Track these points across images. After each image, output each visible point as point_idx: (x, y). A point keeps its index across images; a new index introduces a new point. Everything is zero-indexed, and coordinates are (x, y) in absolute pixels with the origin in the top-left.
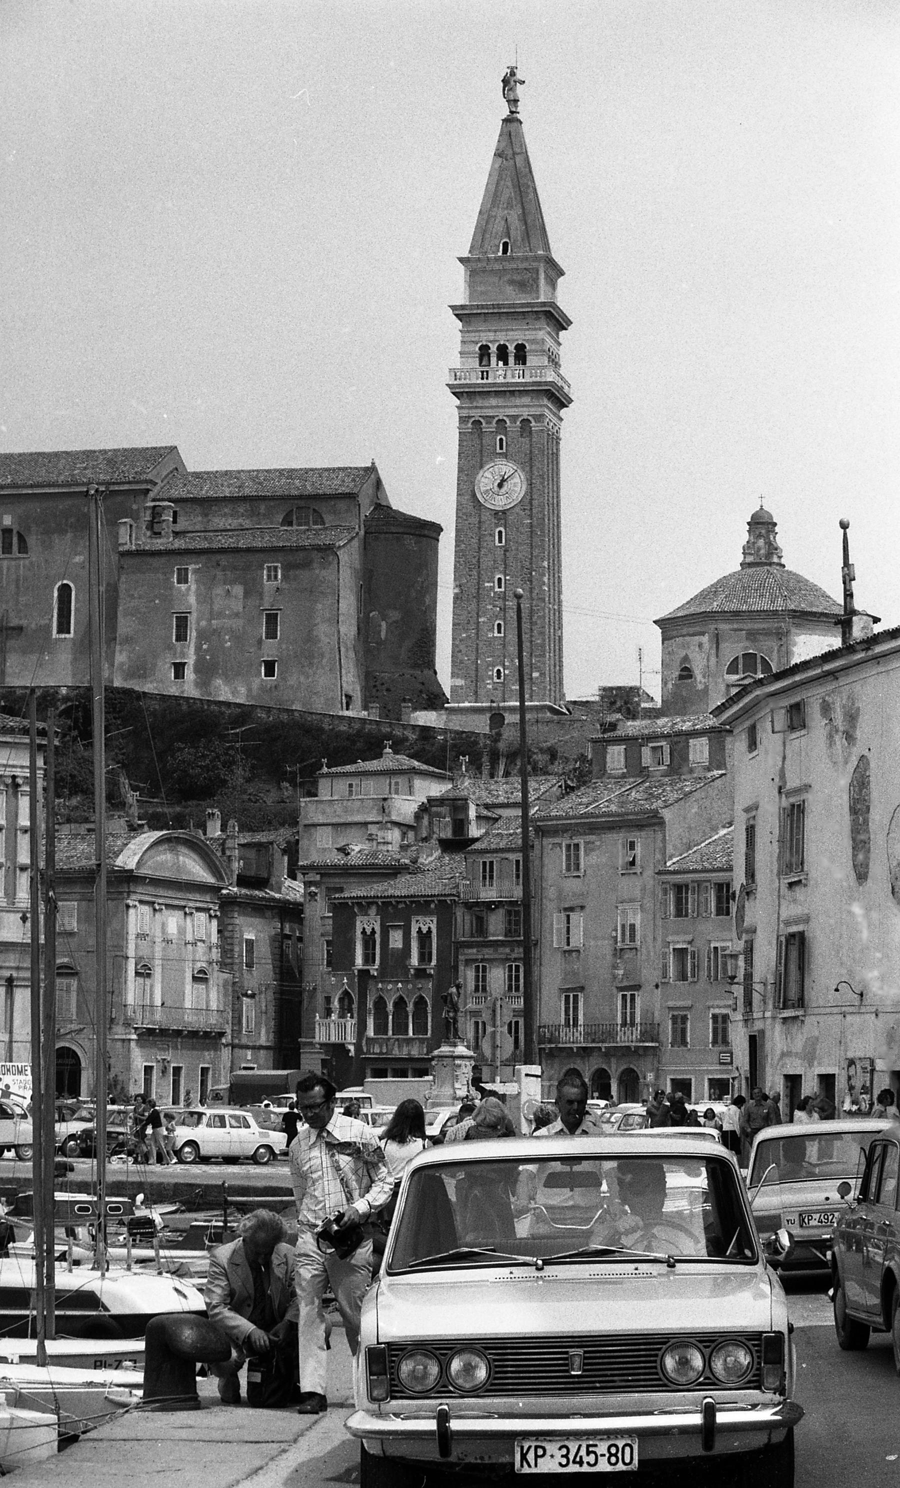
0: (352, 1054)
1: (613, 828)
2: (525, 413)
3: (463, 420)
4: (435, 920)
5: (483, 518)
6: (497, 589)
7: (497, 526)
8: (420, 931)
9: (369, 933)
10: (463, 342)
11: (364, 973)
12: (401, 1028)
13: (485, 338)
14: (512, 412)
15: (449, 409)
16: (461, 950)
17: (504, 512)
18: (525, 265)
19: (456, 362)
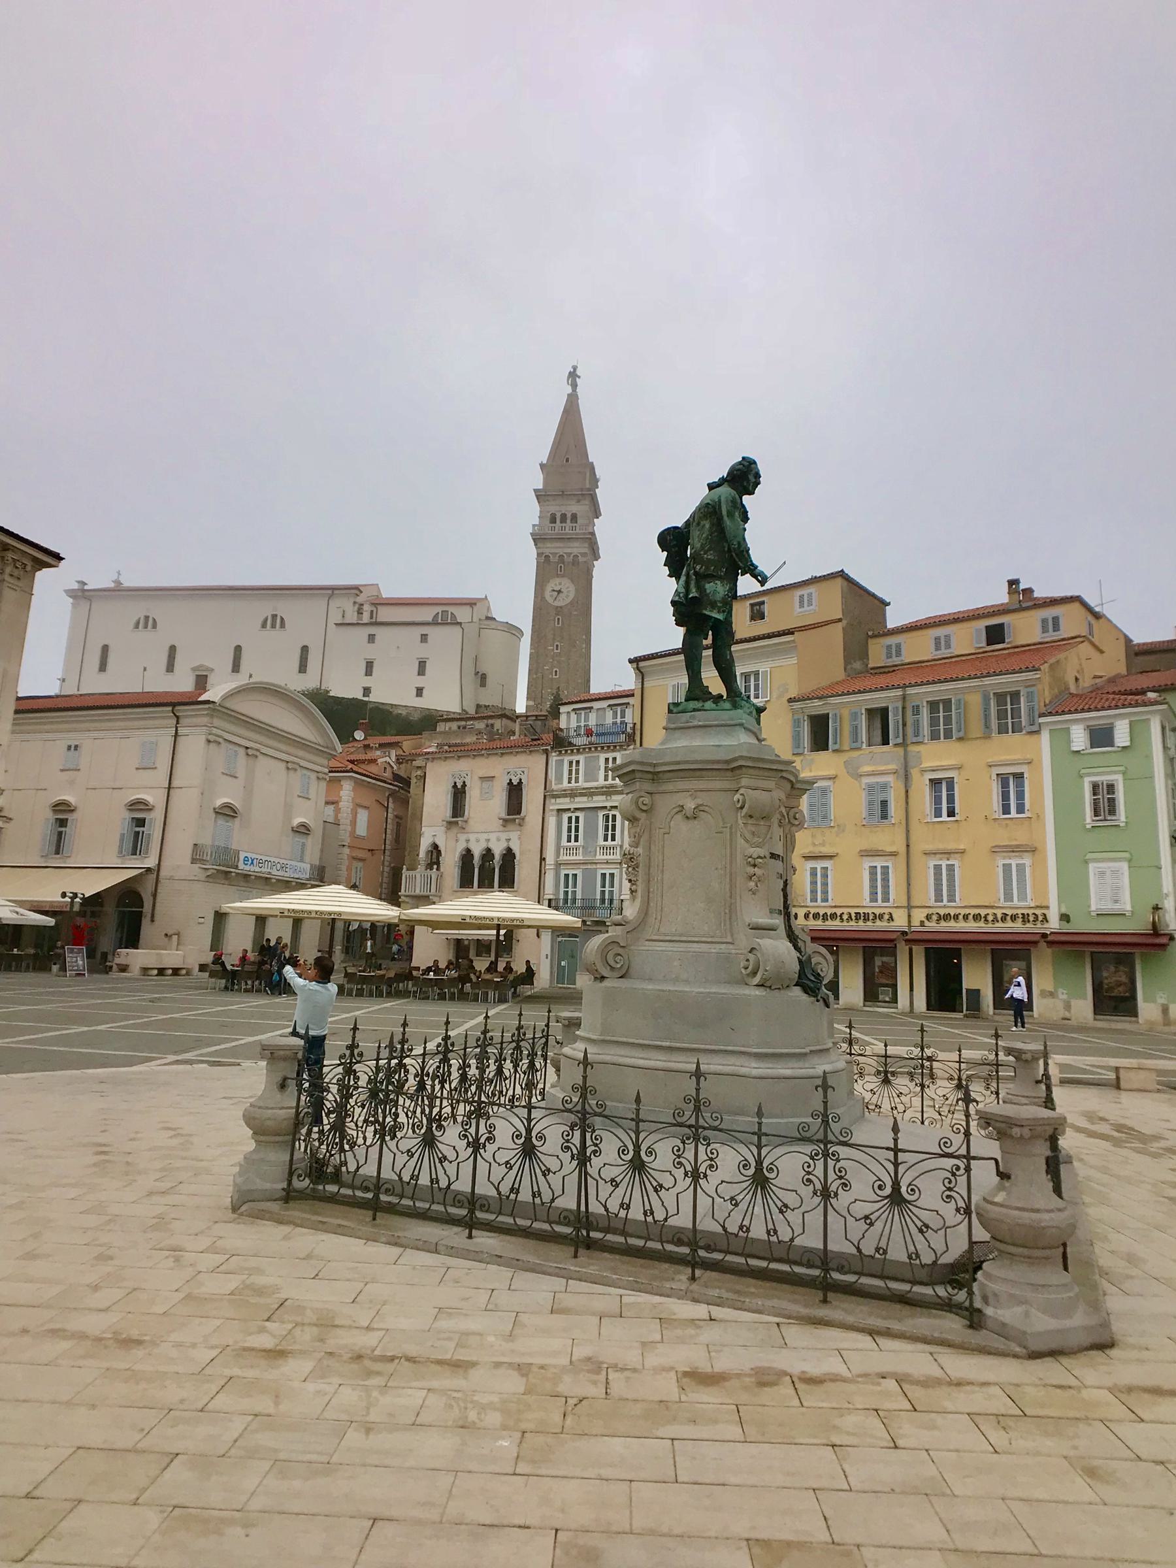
2: (575, 551)
14: (569, 551)
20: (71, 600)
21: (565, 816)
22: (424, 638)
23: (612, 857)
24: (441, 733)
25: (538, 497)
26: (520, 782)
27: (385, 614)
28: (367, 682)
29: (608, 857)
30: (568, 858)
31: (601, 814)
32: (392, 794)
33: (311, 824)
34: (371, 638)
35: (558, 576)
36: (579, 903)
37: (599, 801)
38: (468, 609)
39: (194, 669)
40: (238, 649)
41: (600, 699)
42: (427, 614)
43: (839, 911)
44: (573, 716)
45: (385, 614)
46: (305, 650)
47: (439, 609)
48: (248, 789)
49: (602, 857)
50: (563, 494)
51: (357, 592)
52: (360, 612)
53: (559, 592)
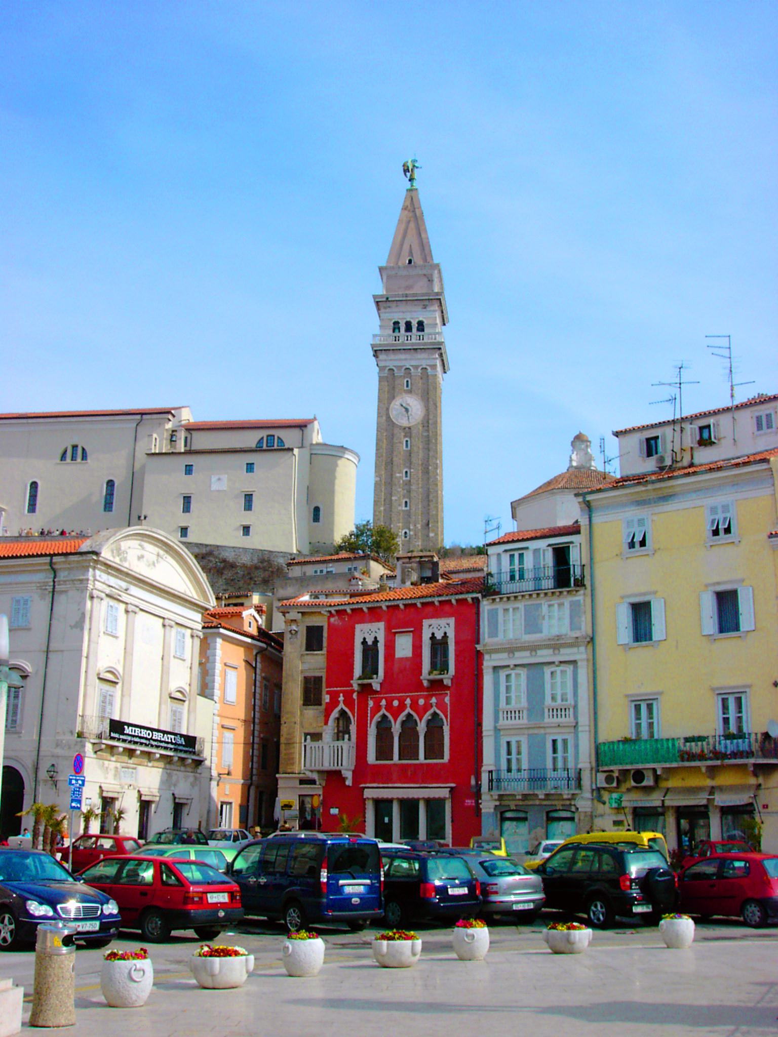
0: (349, 782)
1: (699, 490)
2: (424, 364)
3: (381, 369)
4: (452, 621)
5: (395, 432)
6: (404, 478)
7: (405, 436)
8: (433, 637)
9: (370, 642)
11: (366, 689)
12: (409, 750)
13: (396, 317)
14: (414, 363)
16: (486, 657)
17: (409, 428)
18: (425, 272)
19: (377, 331)
21: (503, 674)
22: (250, 467)
23: (563, 719)
24: (296, 579)
25: (377, 303)
26: (445, 636)
27: (202, 441)
29: (559, 720)
30: (509, 722)
31: (547, 671)
32: (261, 651)
33: (187, 688)
34: (189, 469)
36: (524, 774)
37: (544, 655)
38: (296, 432)
40: (34, 485)
41: (536, 538)
42: (250, 439)
44: (505, 558)
45: (202, 441)
46: (110, 484)
47: (264, 433)
48: (128, 651)
49: (551, 720)
50: (407, 300)
51: (170, 417)
52: (172, 440)
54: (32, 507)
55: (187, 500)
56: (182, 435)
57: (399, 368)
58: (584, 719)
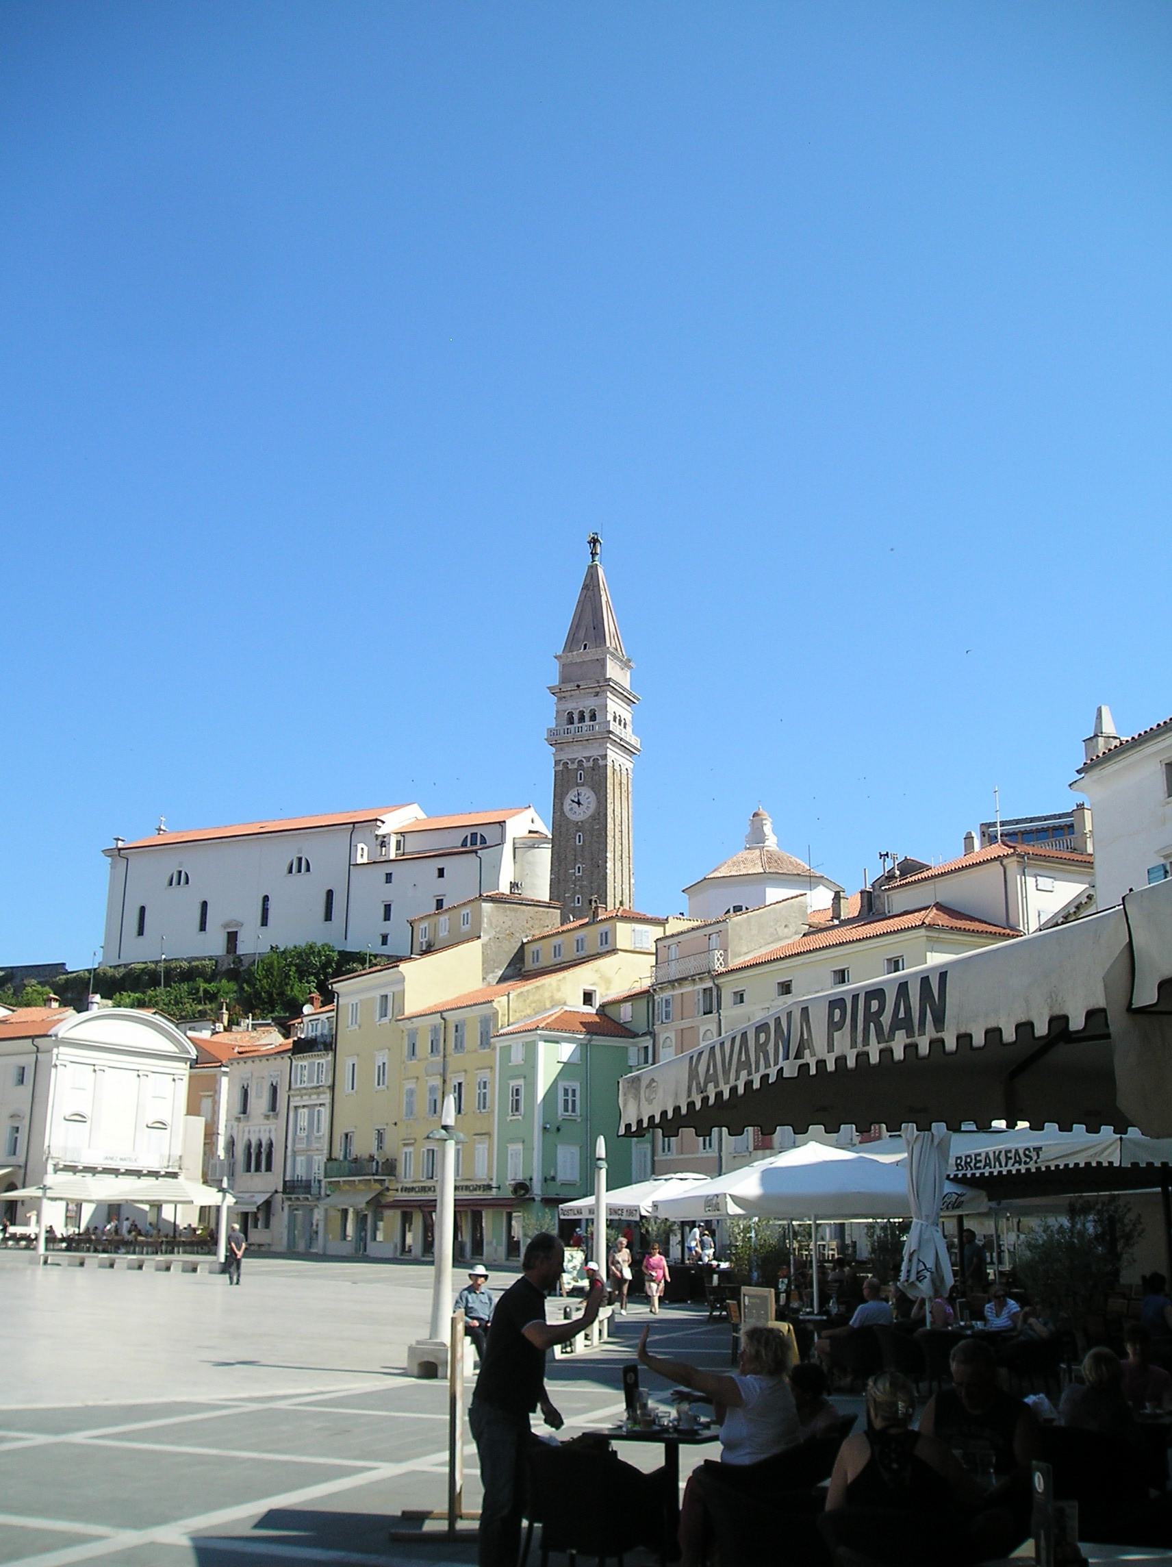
3: (557, 763)
10: (557, 712)
15: (548, 756)
20: (110, 859)
21: (301, 1111)
22: (441, 873)
27: (412, 846)
28: (386, 927)
33: (167, 1120)
34: (389, 878)
35: (578, 785)
37: (314, 1100)
39: (226, 926)
40: (266, 899)
42: (455, 841)
43: (415, 1185)
46: (330, 894)
51: (379, 823)
53: (579, 803)
54: (264, 922)
55: (388, 908)
56: (393, 841)
57: (573, 761)
58: (326, 1146)
